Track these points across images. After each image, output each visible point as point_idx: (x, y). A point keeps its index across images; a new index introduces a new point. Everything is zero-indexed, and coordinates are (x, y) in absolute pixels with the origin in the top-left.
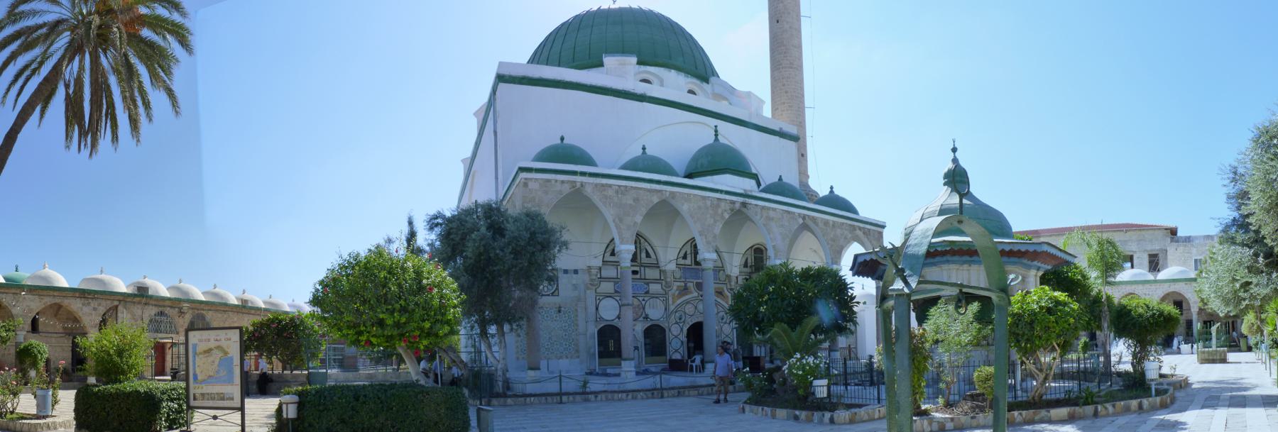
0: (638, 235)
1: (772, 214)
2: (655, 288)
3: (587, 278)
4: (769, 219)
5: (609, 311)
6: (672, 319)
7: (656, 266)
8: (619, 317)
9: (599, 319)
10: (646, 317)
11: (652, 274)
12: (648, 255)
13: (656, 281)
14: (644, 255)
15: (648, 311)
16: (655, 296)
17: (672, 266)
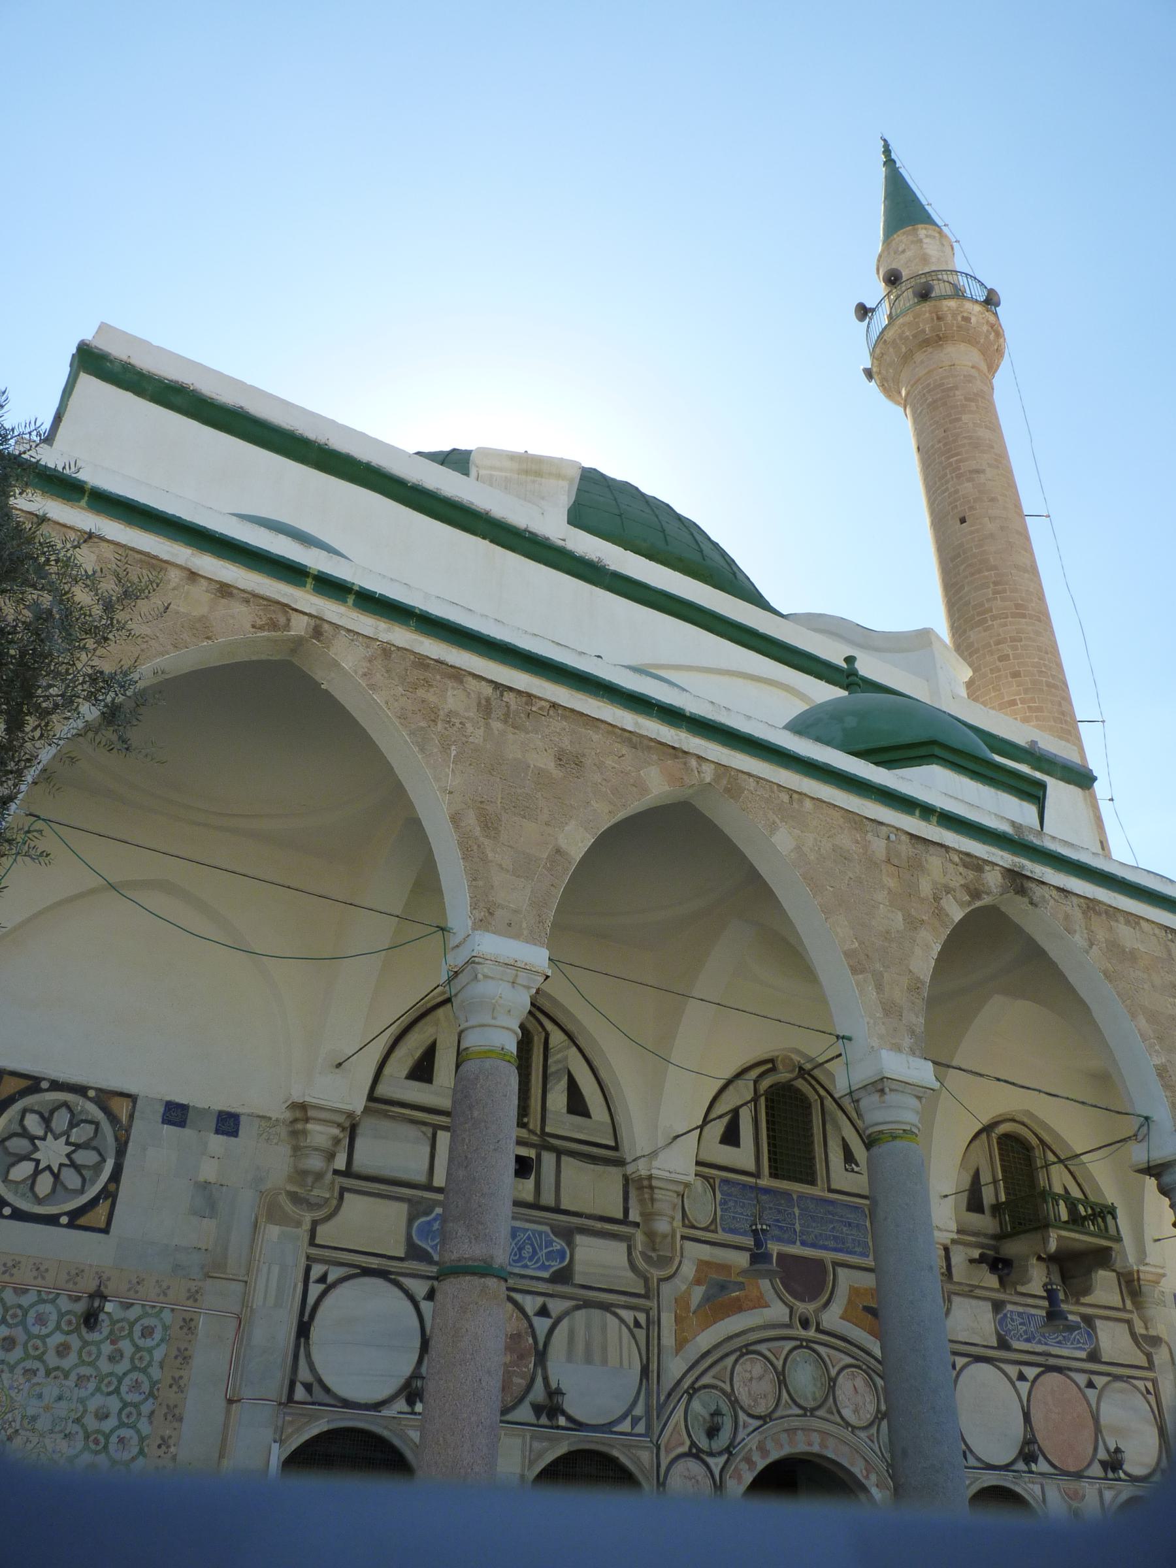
0: (539, 1010)
1: (1126, 935)
2: (599, 1258)
3: (276, 1162)
4: (1114, 947)
5: (363, 1350)
6: (677, 1430)
7: (609, 1155)
8: (411, 1391)
9: (302, 1387)
10: (551, 1408)
11: (587, 1189)
12: (577, 1105)
13: (606, 1227)
14: (558, 1099)
15: (561, 1371)
16: (596, 1300)
17: (677, 1164)
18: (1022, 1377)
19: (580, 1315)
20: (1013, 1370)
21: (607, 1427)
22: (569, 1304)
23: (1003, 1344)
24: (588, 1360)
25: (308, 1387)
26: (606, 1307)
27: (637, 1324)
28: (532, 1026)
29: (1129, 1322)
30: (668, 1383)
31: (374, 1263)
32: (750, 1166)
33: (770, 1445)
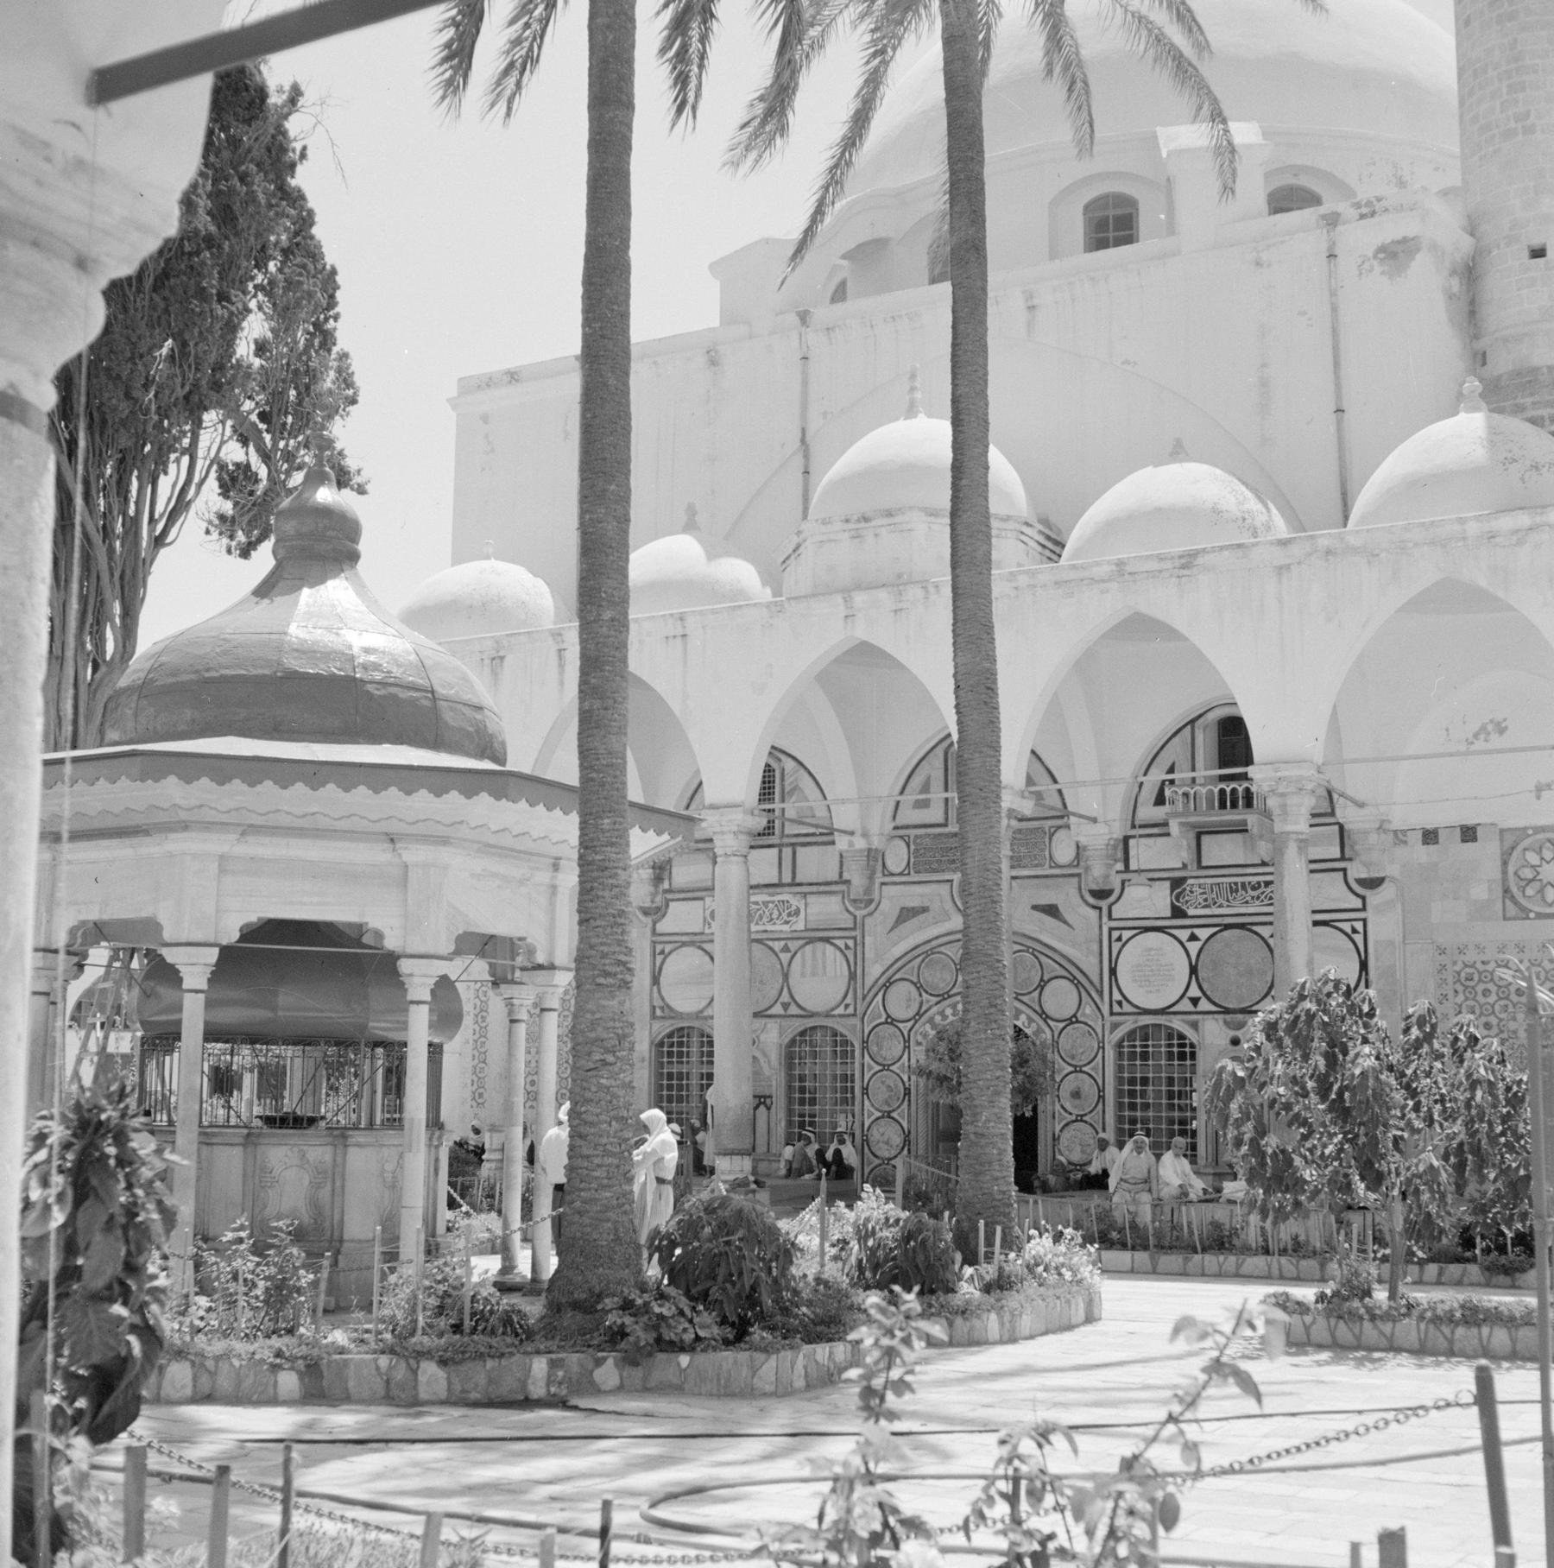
18: (1193, 938)
19: (808, 948)
20: (1184, 935)
21: (828, 1015)
22: (801, 942)
23: (1177, 912)
24: (814, 974)
25: (662, 1008)
26: (827, 940)
27: (847, 947)
28: (774, 765)
29: (1344, 870)
30: (869, 982)
31: (684, 939)
32: (940, 819)
33: (949, 1012)
